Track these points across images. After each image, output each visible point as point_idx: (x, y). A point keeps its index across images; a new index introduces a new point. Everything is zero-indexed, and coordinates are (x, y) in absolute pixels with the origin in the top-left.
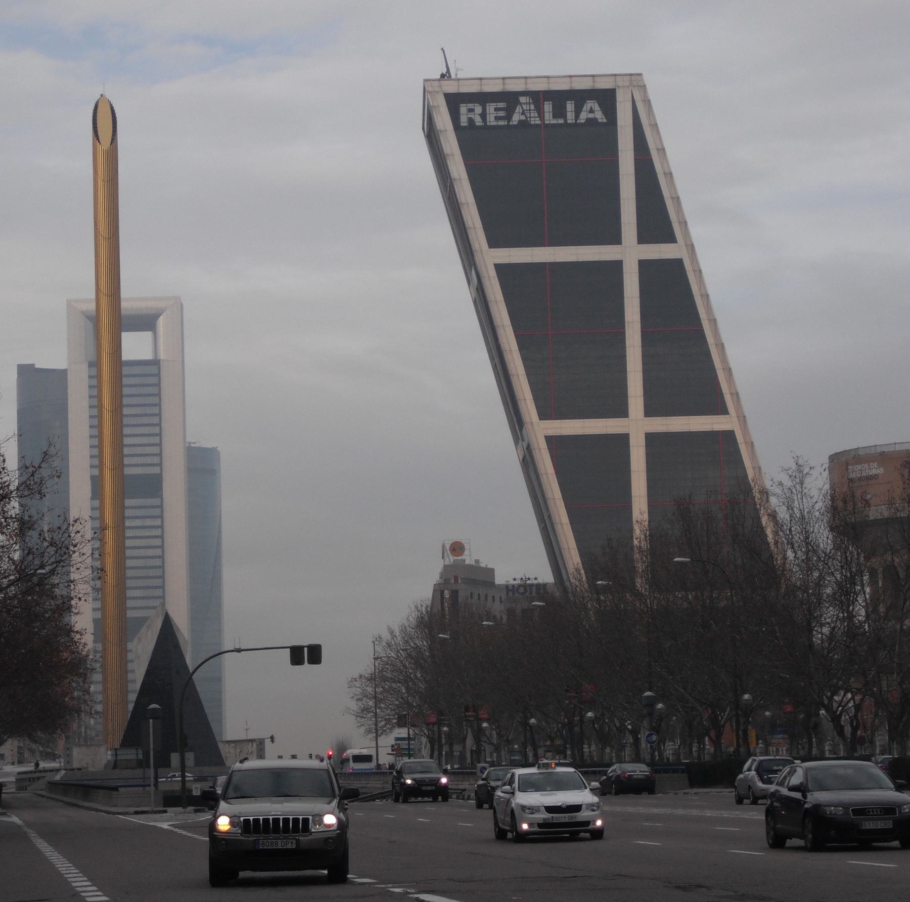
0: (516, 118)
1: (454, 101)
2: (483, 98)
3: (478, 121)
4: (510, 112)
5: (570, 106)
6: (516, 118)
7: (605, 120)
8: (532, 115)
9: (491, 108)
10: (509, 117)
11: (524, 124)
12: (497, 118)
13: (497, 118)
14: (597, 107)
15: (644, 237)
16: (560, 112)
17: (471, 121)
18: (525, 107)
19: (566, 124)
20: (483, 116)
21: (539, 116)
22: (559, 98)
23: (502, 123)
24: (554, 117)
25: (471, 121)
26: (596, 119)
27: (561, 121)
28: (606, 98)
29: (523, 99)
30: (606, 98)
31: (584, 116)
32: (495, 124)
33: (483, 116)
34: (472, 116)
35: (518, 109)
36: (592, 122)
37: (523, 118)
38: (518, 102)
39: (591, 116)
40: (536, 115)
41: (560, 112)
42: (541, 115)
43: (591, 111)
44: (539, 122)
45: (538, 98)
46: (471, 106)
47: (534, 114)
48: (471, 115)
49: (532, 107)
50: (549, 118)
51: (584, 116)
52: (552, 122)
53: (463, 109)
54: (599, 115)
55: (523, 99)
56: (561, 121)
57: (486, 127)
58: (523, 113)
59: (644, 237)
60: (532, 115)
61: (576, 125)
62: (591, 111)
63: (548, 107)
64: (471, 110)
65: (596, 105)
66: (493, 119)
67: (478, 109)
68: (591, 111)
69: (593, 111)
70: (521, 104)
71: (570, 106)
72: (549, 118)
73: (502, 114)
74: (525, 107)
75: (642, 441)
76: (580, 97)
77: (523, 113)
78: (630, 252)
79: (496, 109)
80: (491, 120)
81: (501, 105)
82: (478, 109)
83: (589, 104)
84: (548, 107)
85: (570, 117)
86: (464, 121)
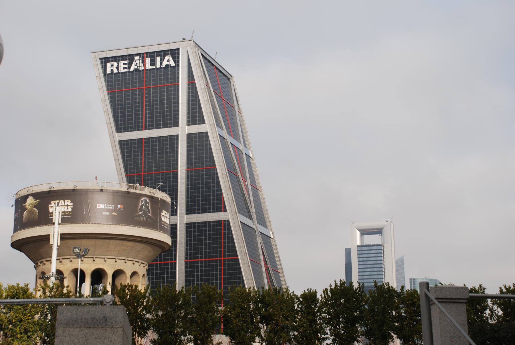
1: (104, 61)
2: (117, 59)
3: (115, 71)
4: (130, 64)
5: (158, 59)
7: (174, 65)
9: (121, 63)
10: (129, 68)
11: (136, 70)
12: (124, 68)
15: (190, 122)
16: (153, 63)
17: (112, 70)
18: (137, 62)
19: (157, 69)
20: (118, 68)
21: (144, 66)
22: (153, 55)
23: (127, 70)
27: (154, 67)
28: (175, 53)
29: (136, 58)
30: (175, 53)
33: (118, 68)
35: (134, 63)
37: (136, 67)
38: (133, 59)
39: (168, 63)
41: (153, 63)
42: (144, 65)
45: (143, 56)
46: (112, 63)
47: (142, 65)
48: (112, 68)
49: (141, 61)
51: (165, 64)
53: (109, 65)
54: (172, 63)
55: (136, 58)
56: (154, 67)
57: (119, 73)
58: (136, 65)
61: (161, 68)
63: (148, 60)
64: (112, 66)
65: (171, 57)
67: (115, 64)
68: (168, 61)
69: (169, 60)
71: (158, 59)
72: (148, 66)
73: (127, 66)
75: (184, 228)
76: (163, 54)
77: (136, 65)
79: (124, 64)
80: (121, 70)
81: (127, 62)
84: (148, 60)
85: (158, 65)
86: (109, 71)
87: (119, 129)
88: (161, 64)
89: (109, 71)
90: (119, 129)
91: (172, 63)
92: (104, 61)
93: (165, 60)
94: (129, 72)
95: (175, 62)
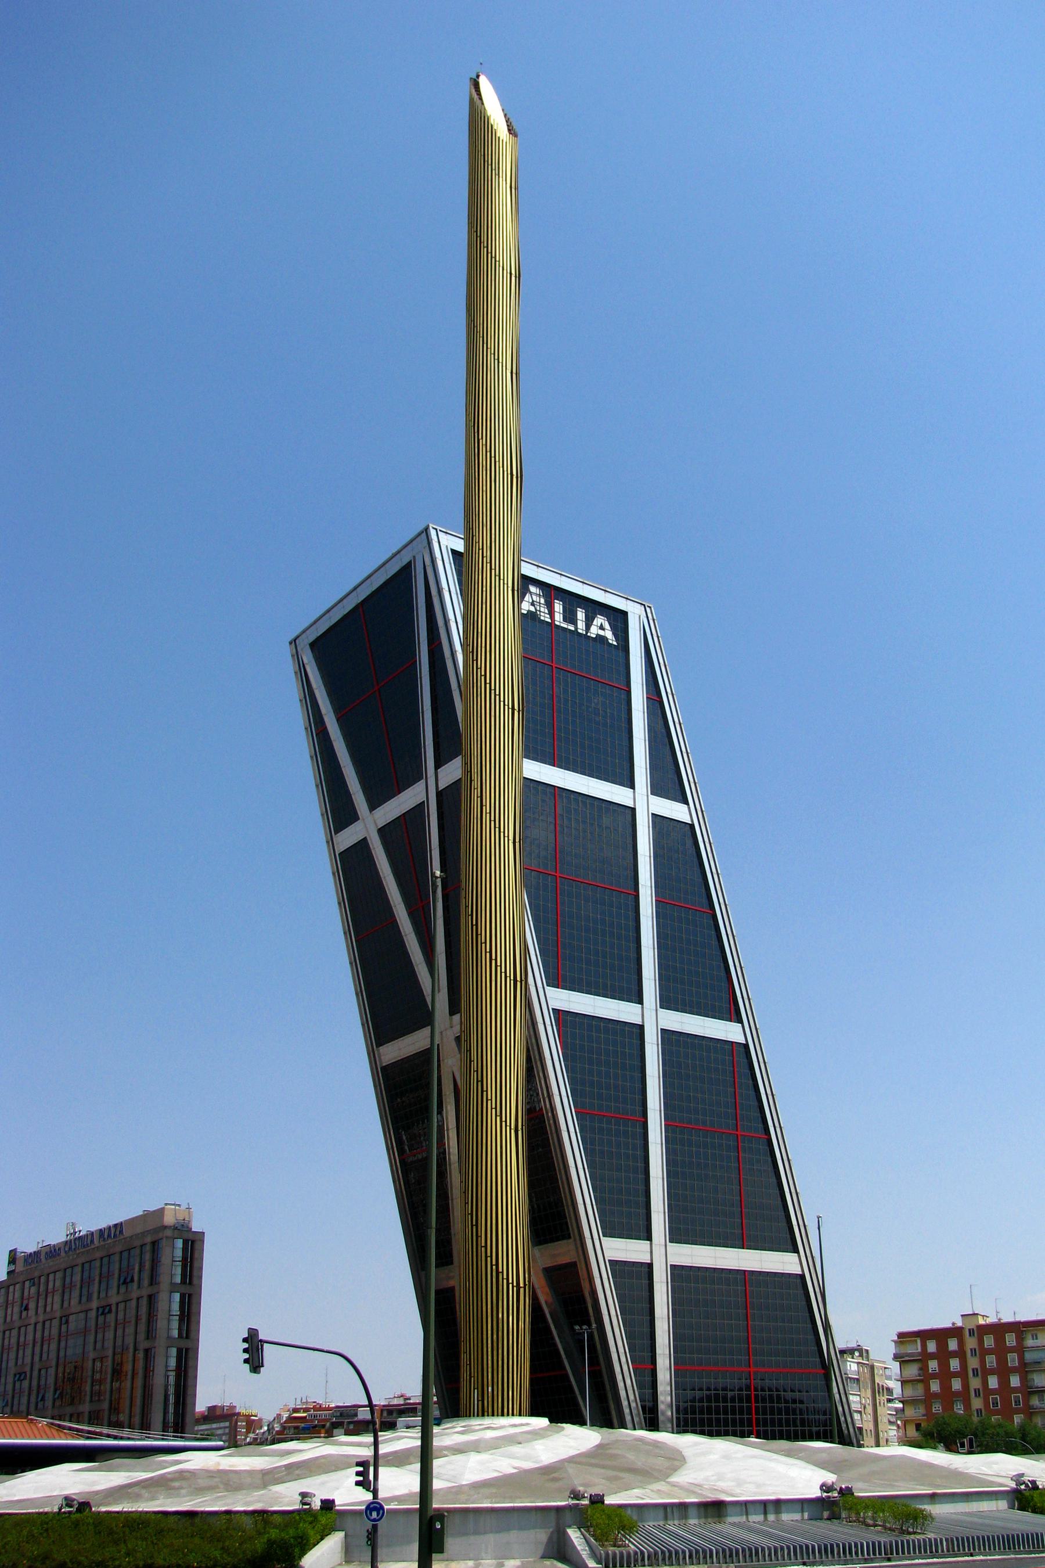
5: (581, 615)
14: (607, 626)
18: (535, 598)
24: (565, 620)
29: (533, 589)
31: (594, 631)
35: (527, 597)
36: (601, 639)
37: (532, 609)
39: (601, 633)
42: (551, 613)
43: (602, 628)
49: (542, 601)
50: (559, 618)
51: (594, 631)
54: (609, 634)
58: (533, 604)
59: (658, 789)
60: (542, 609)
62: (602, 628)
63: (558, 607)
69: (601, 628)
70: (531, 593)
71: (581, 615)
74: (535, 598)
78: (646, 803)
83: (600, 620)
84: (558, 607)
88: (588, 627)
91: (609, 634)
93: (595, 622)
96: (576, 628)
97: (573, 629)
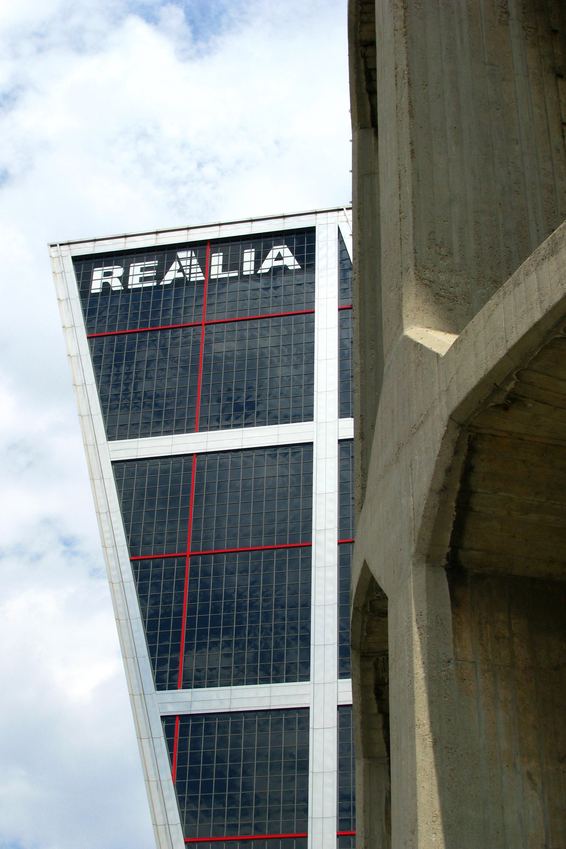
0: (170, 276)
1: (84, 264)
3: (116, 285)
5: (249, 256)
6: (170, 276)
7: (299, 267)
8: (193, 271)
9: (136, 270)
10: (159, 277)
13: (142, 280)
14: (286, 252)
17: (106, 286)
18: (183, 263)
19: (243, 278)
20: (124, 279)
22: (232, 246)
25: (106, 286)
26: (286, 267)
27: (235, 274)
29: (181, 255)
31: (267, 265)
32: (140, 286)
33: (124, 279)
34: (109, 281)
35: (175, 266)
37: (180, 275)
39: (279, 263)
40: (199, 270)
44: (203, 278)
45: (203, 248)
46: (108, 269)
49: (195, 261)
51: (267, 265)
52: (220, 276)
53: (98, 274)
54: (290, 262)
56: (235, 274)
57: (126, 290)
58: (181, 270)
61: (256, 276)
63: (217, 260)
66: (136, 280)
67: (118, 271)
70: (179, 260)
71: (249, 256)
72: (216, 271)
73: (151, 273)
76: (262, 242)
77: (181, 270)
79: (142, 270)
80: (134, 282)
81: (153, 263)
82: (118, 271)
84: (217, 260)
85: (248, 268)
86: (96, 286)
87: (114, 432)
89: (96, 286)
90: (114, 432)
92: (84, 264)
93: (269, 256)
94: (158, 287)
95: (299, 259)
96: (241, 270)
97: (236, 274)
